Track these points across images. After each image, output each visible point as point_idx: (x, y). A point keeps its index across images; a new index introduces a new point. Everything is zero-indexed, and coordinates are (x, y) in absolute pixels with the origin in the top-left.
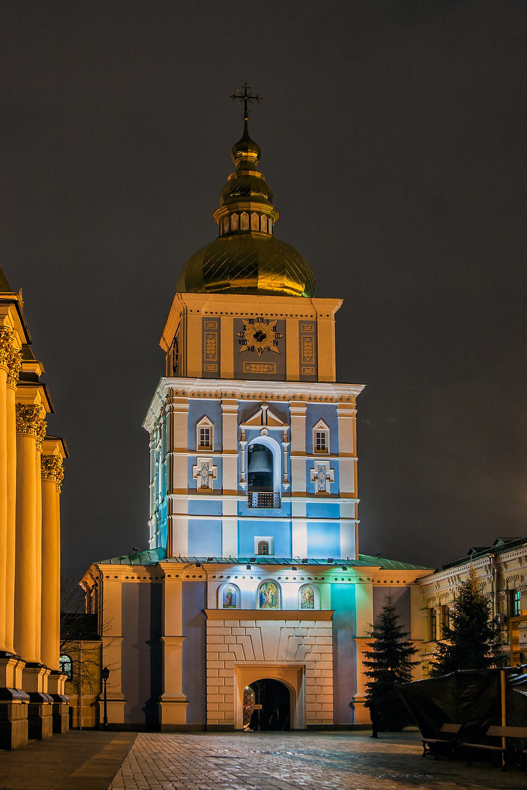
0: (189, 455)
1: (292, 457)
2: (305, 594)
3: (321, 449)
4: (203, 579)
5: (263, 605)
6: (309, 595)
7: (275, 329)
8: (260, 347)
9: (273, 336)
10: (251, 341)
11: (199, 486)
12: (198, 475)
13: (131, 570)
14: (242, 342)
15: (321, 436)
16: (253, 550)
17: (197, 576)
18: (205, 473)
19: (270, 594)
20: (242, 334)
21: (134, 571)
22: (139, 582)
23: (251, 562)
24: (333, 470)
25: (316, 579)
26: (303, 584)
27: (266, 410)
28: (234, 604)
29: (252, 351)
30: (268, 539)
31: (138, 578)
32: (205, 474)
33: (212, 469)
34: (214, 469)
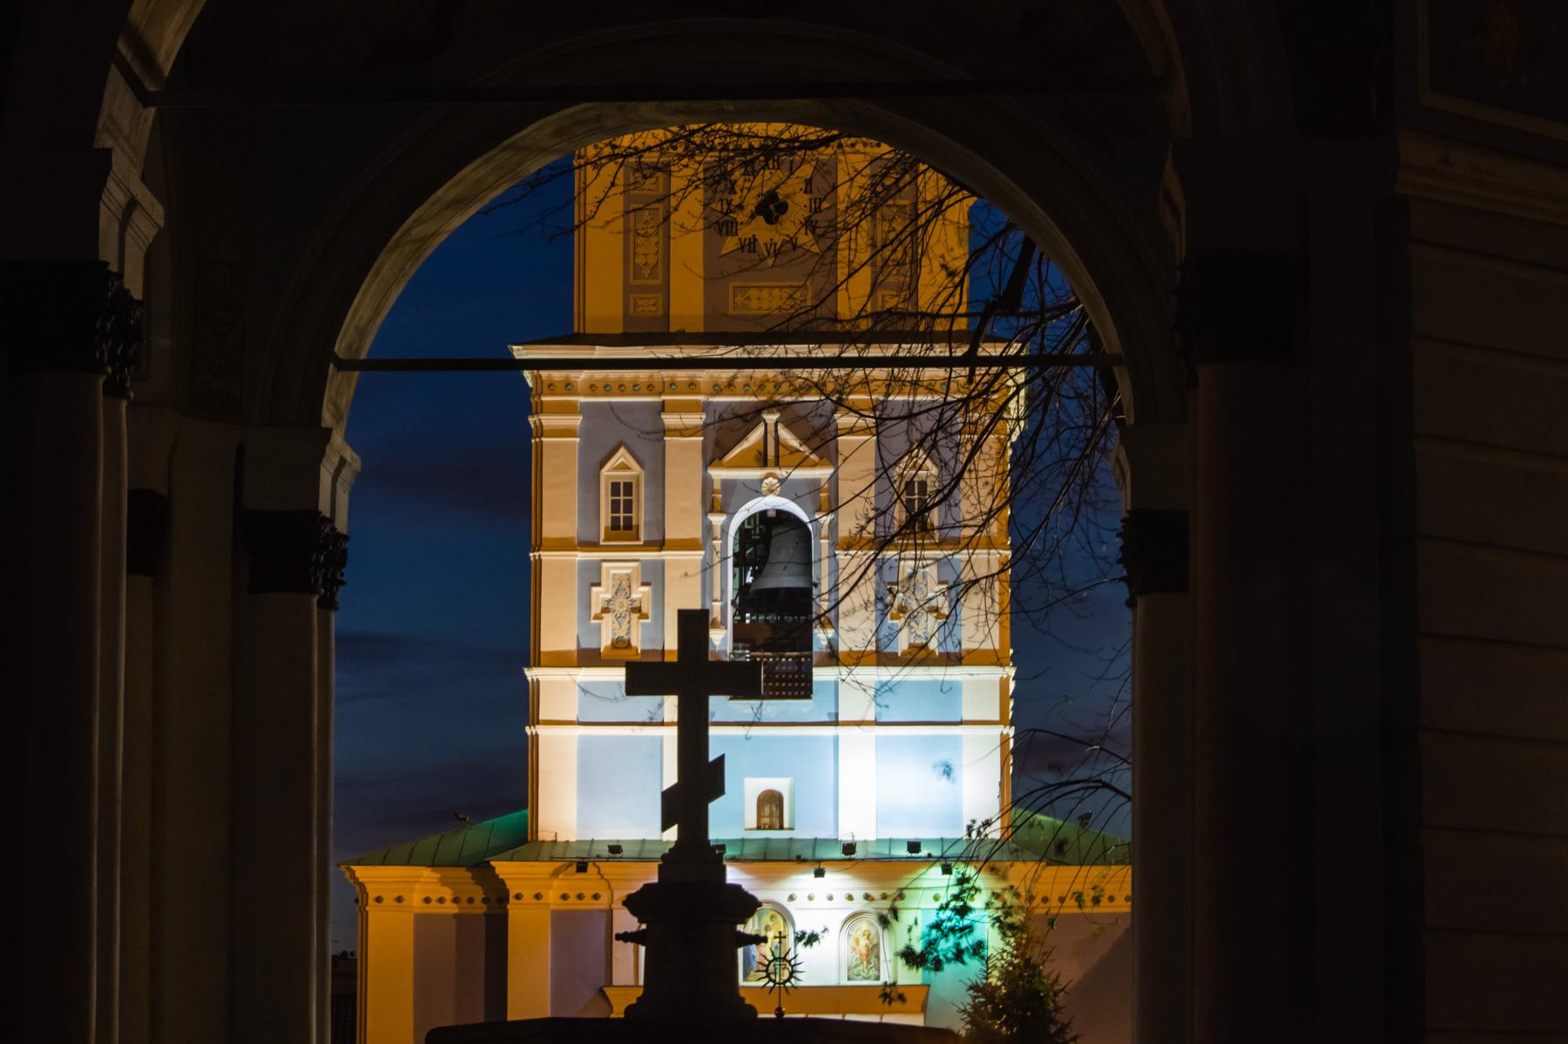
0: (581, 556)
2: (857, 942)
7: (809, 187)
8: (771, 240)
9: (805, 206)
11: (606, 641)
12: (606, 610)
13: (436, 880)
14: (724, 229)
18: (621, 605)
20: (725, 207)
21: (444, 882)
22: (456, 911)
26: (849, 912)
27: (776, 424)
29: (750, 251)
31: (455, 900)
32: (622, 607)
33: (640, 593)
34: (644, 593)
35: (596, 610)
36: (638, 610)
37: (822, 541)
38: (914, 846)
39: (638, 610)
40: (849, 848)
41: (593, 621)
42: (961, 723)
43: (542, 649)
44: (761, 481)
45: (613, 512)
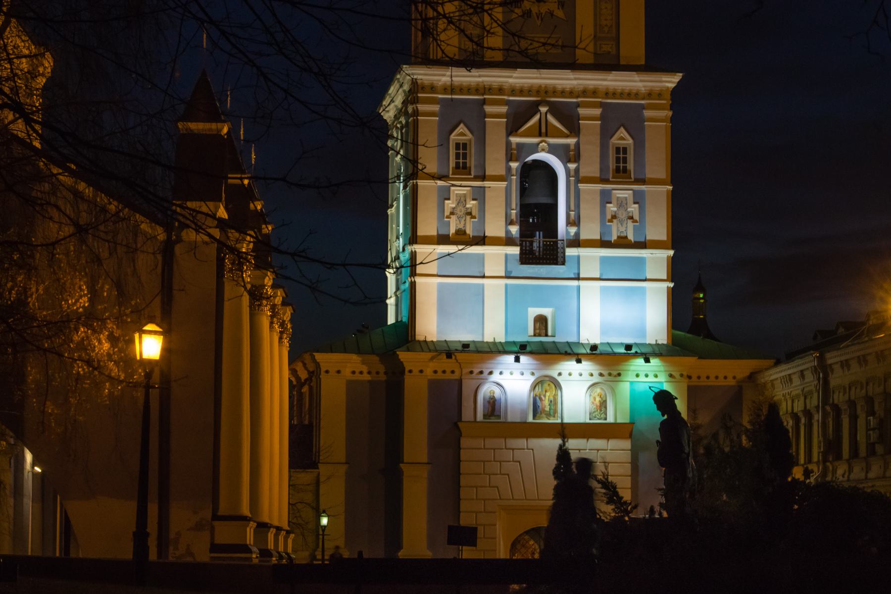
1: (581, 186)
2: (595, 399)
3: (621, 174)
4: (456, 376)
5: (538, 415)
6: (600, 399)
11: (452, 230)
12: (452, 213)
13: (359, 361)
15: (621, 151)
16: (526, 328)
17: (448, 371)
18: (460, 211)
19: (547, 397)
21: (363, 363)
22: (370, 379)
23: (521, 351)
24: (636, 206)
25: (610, 374)
26: (591, 383)
27: (546, 113)
28: (498, 414)
30: (547, 311)
31: (369, 373)
32: (461, 209)
33: (471, 204)
34: (473, 204)
35: (447, 213)
36: (470, 214)
37: (571, 178)
38: (628, 347)
39: (470, 214)
40: (594, 347)
41: (445, 219)
42: (645, 280)
43: (419, 234)
44: (538, 144)
45: (456, 159)
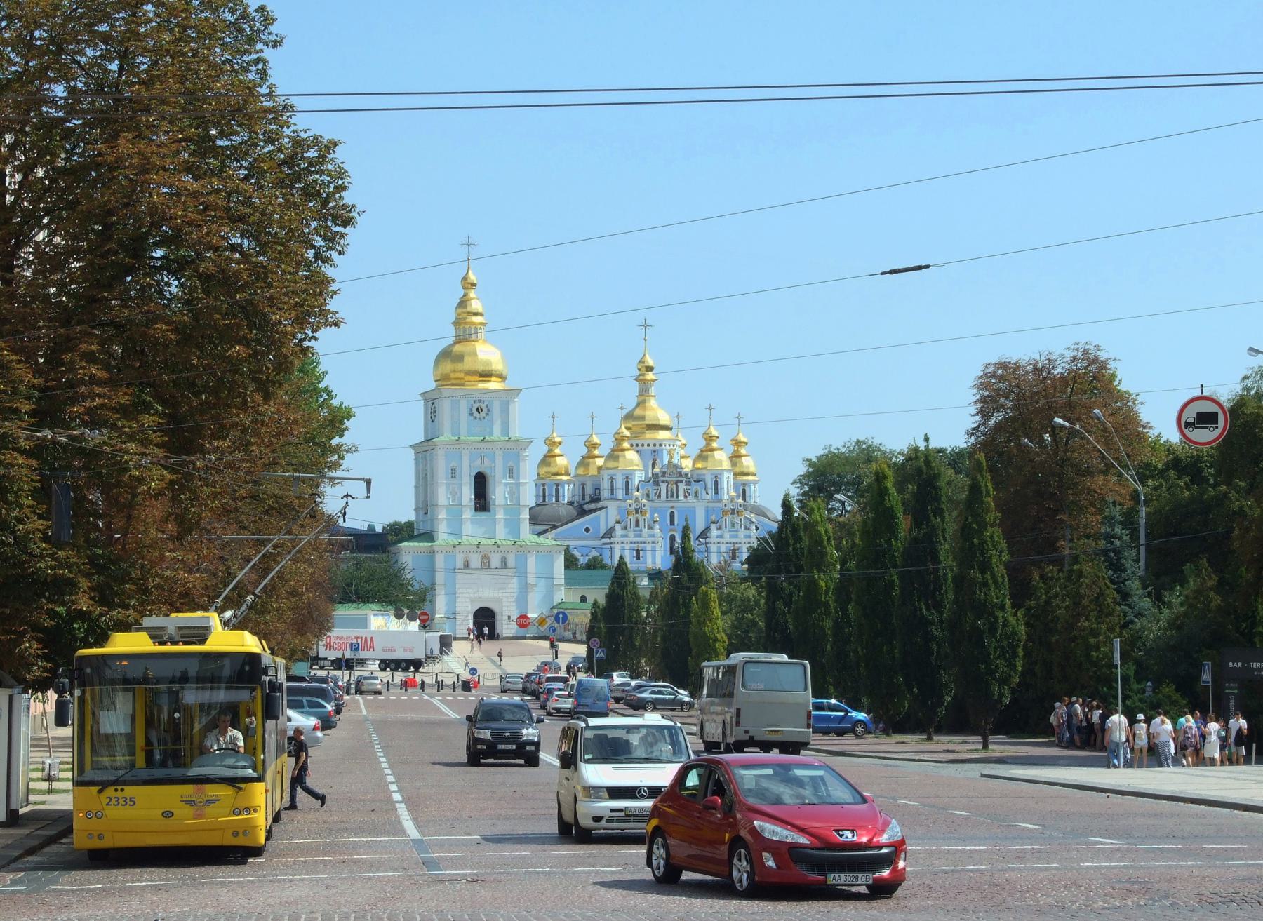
10: (476, 413)
